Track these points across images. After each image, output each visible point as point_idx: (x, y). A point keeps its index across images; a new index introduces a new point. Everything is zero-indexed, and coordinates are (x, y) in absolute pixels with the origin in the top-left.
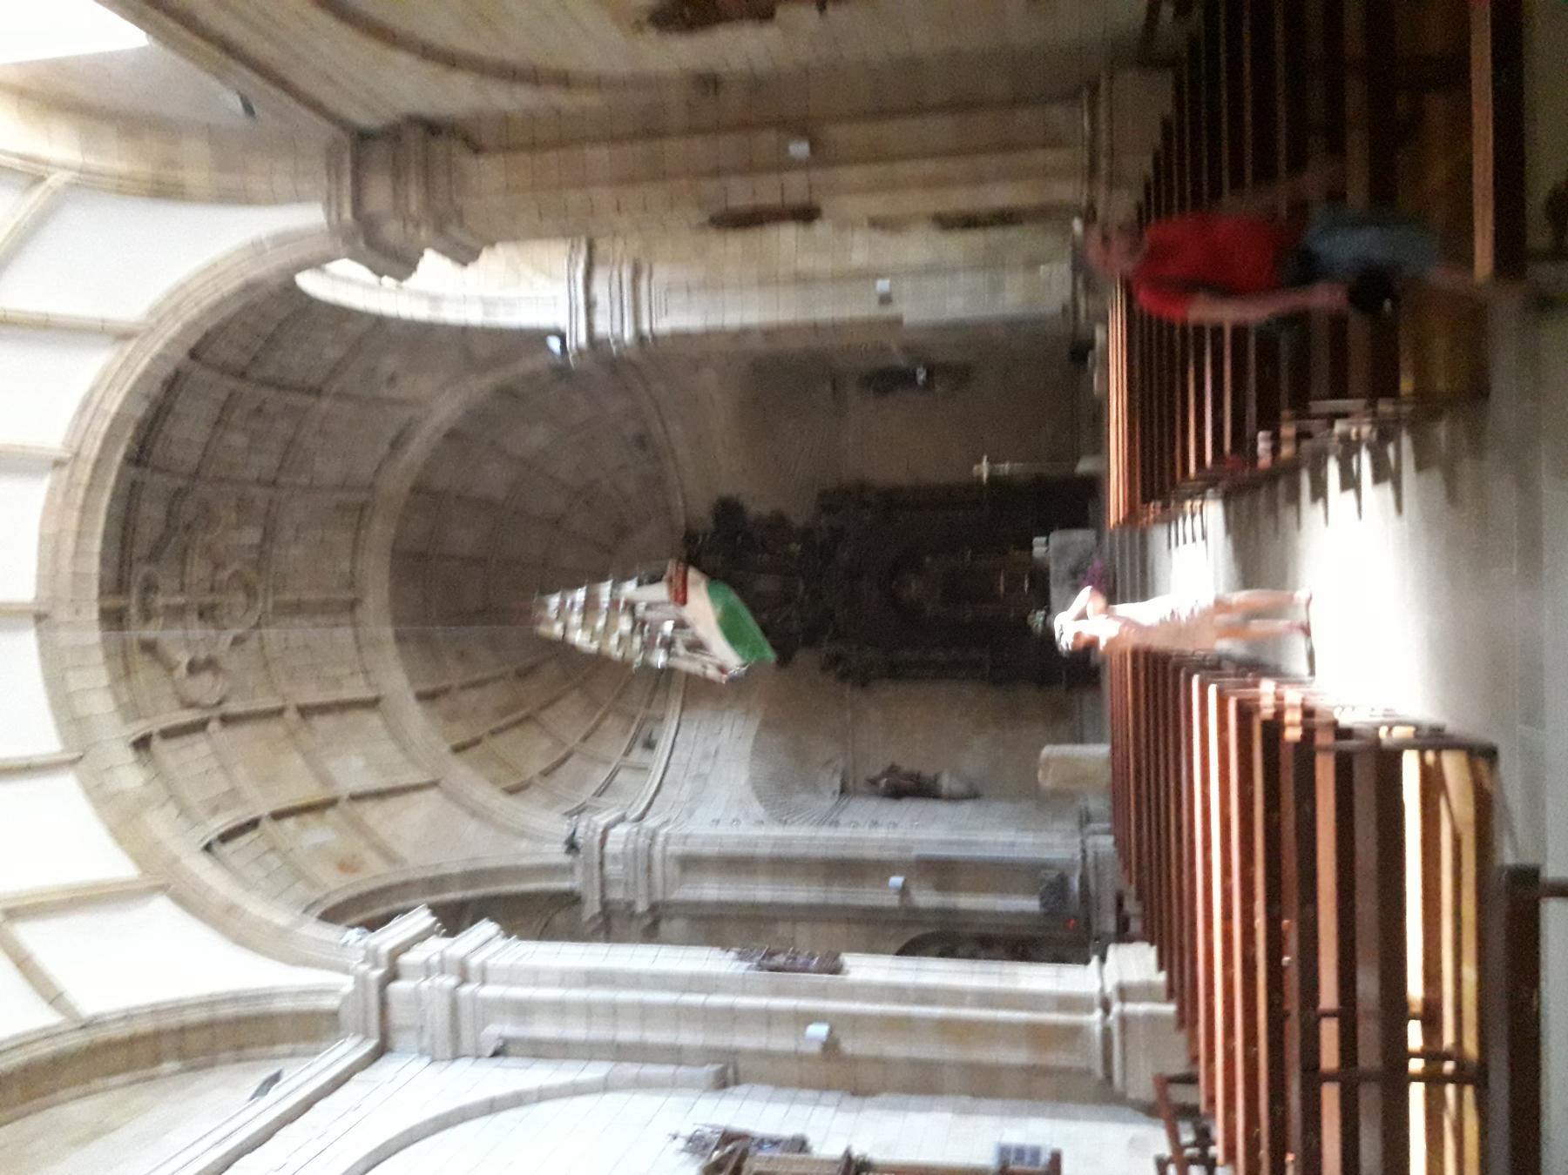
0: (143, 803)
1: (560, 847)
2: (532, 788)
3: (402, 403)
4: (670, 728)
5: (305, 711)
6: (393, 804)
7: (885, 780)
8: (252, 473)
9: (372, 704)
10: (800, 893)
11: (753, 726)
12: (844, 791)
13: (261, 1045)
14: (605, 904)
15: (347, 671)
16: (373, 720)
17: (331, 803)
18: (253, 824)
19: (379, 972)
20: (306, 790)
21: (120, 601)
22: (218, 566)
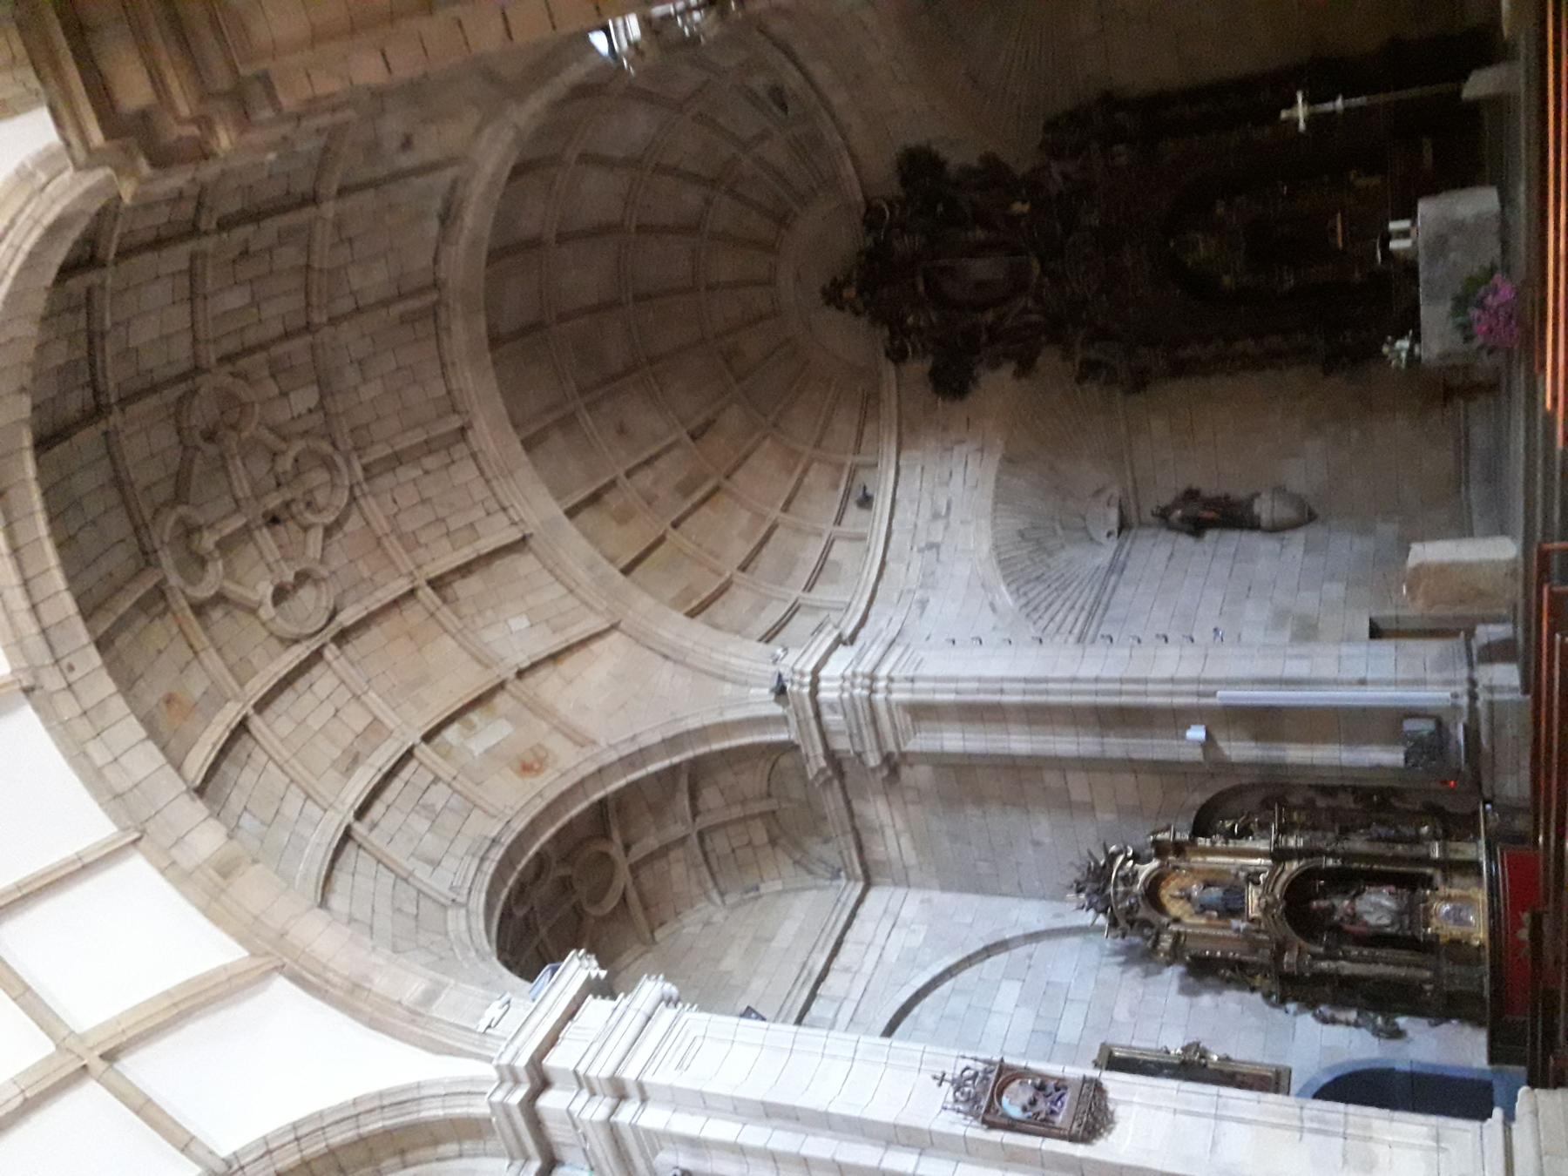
0: (226, 869)
1: (765, 693)
2: (733, 589)
3: (434, 167)
4: (886, 480)
5: (437, 584)
6: (568, 666)
7: (1179, 512)
8: (276, 329)
9: (520, 545)
10: (1065, 744)
11: (992, 463)
12: (1124, 526)
13: (424, 1145)
14: (830, 754)
15: (482, 513)
16: (525, 564)
17: (501, 686)
18: (409, 754)
19: (521, 1093)
20: (468, 682)
21: (149, 582)
22: (275, 455)
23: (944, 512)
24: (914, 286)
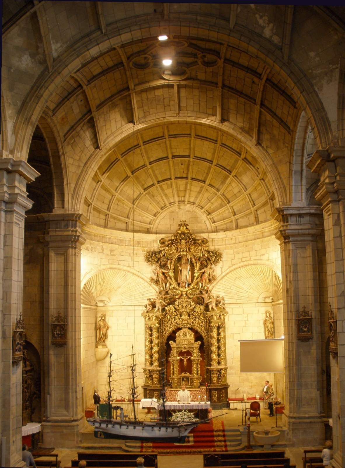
19: (10, 167)
23: (112, 253)
24: (183, 251)
